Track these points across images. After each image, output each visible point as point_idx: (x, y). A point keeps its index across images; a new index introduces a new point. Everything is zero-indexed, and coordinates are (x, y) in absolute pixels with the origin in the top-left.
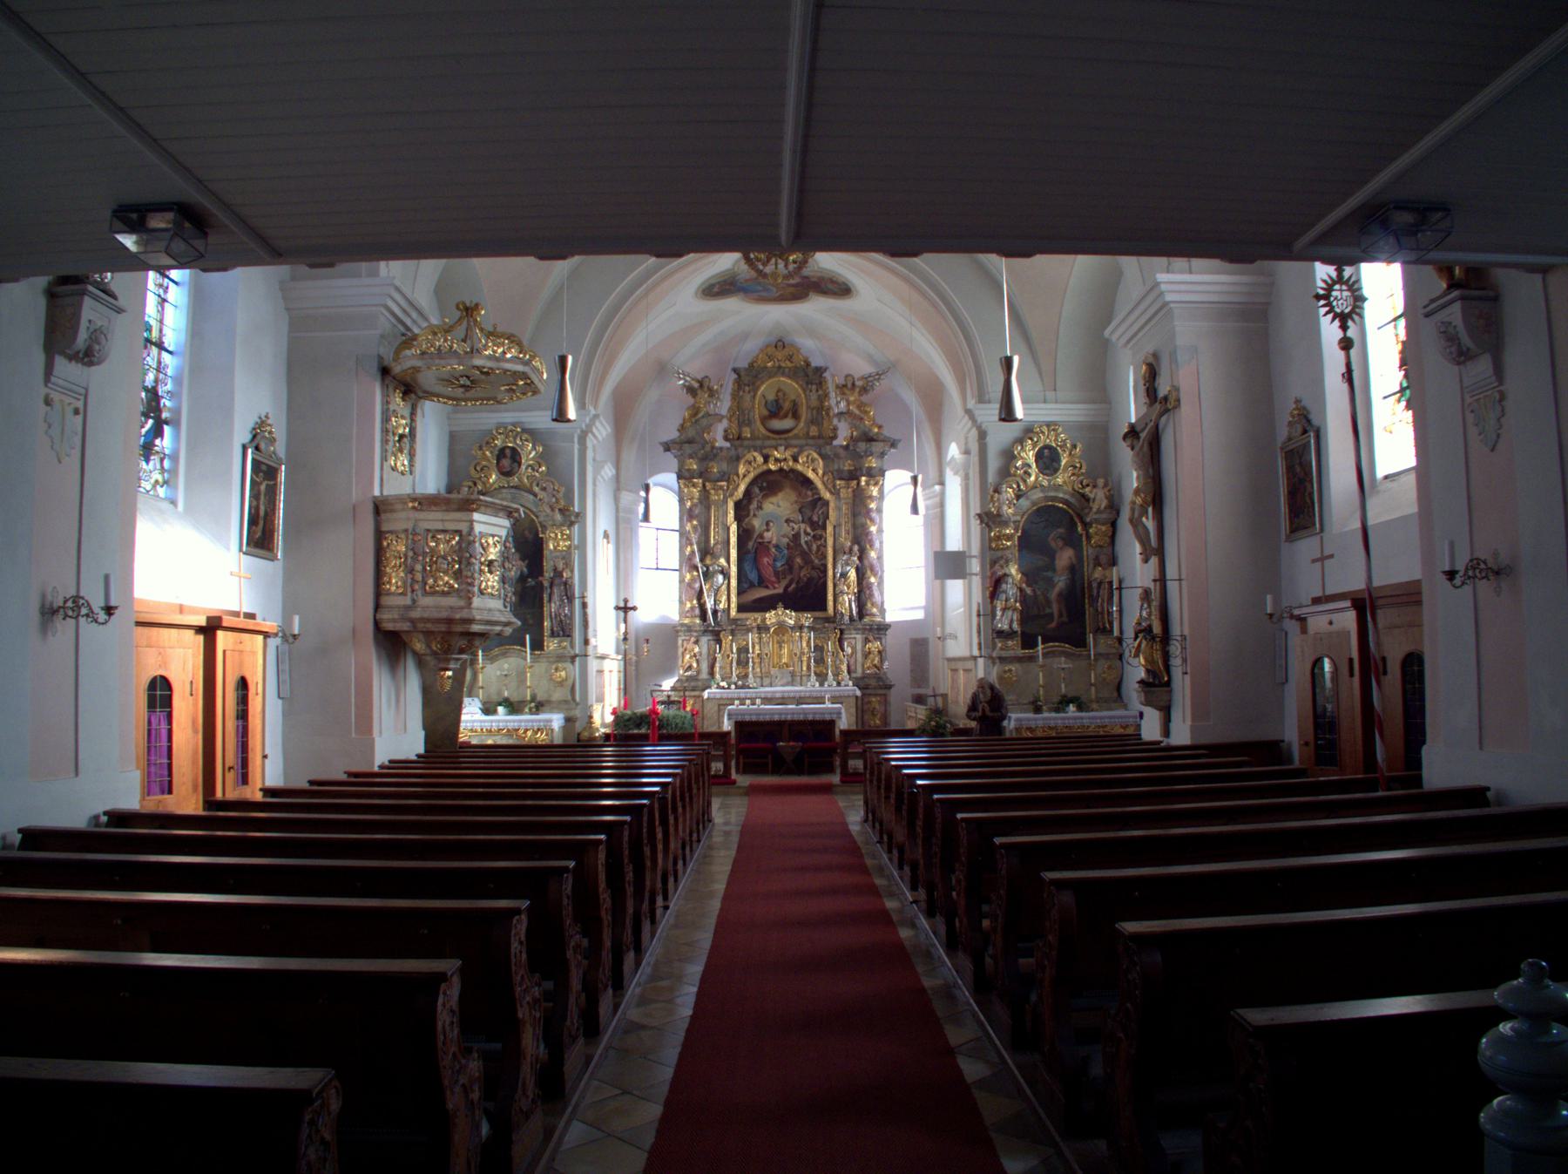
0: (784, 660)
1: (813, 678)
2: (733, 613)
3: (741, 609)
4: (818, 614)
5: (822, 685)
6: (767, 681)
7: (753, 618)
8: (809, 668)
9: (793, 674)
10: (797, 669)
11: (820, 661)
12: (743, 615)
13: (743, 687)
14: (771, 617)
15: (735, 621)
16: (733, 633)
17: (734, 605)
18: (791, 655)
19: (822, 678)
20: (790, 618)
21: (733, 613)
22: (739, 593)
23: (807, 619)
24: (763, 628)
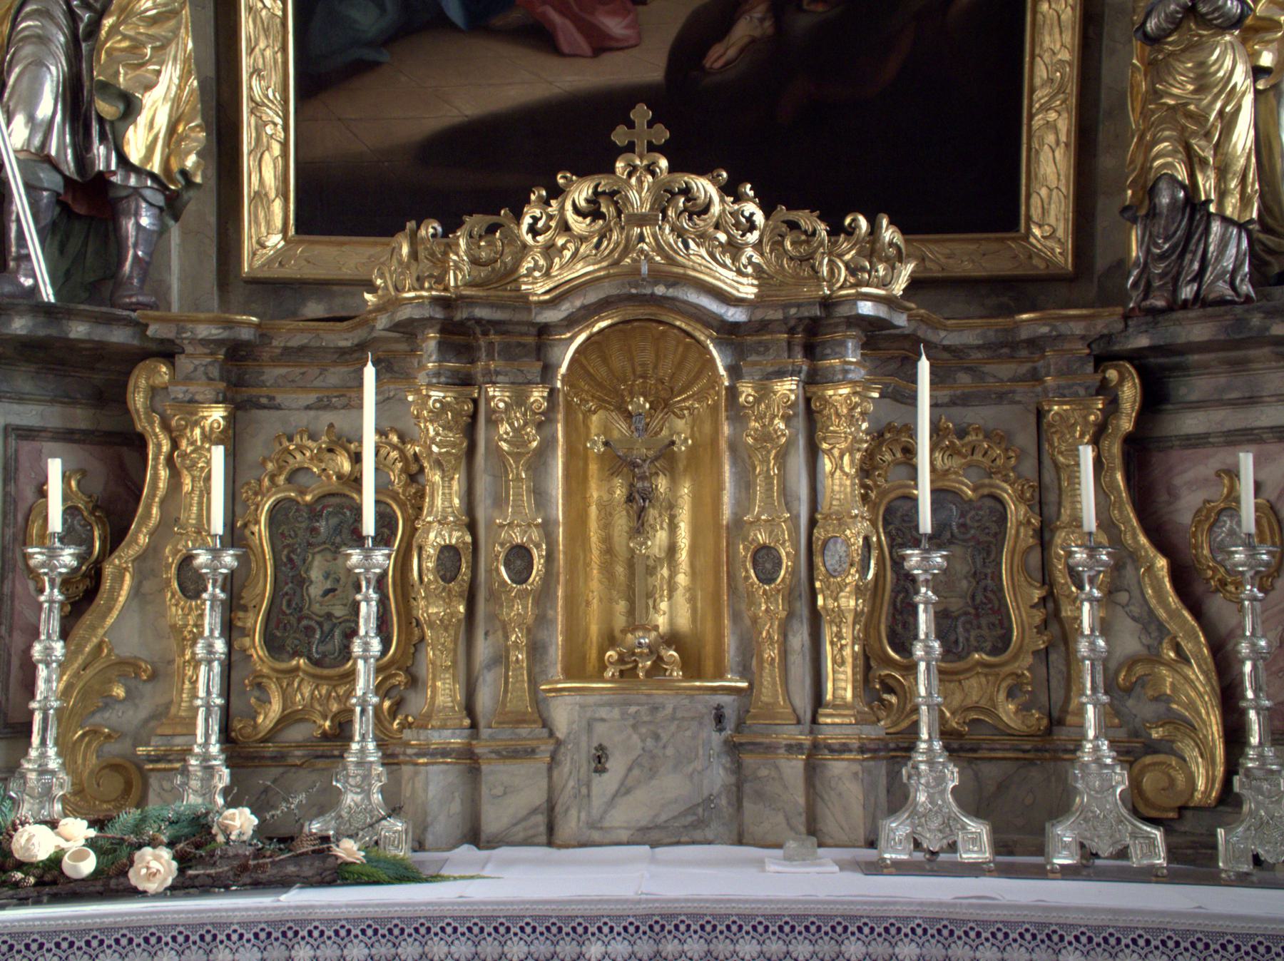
0: (671, 612)
1: (934, 777)
2: (267, 232)
3: (326, 202)
4: (963, 255)
5: (1019, 848)
6: (514, 791)
7: (400, 272)
8: (881, 681)
9: (741, 736)
10: (781, 692)
11: (975, 623)
12: (339, 257)
13: (250, 873)
14: (558, 247)
15: (277, 291)
16: (239, 373)
17: (267, 169)
18: (735, 563)
19: (1017, 784)
20: (727, 250)
21: (267, 232)
22: (316, 80)
23: (875, 268)
24: (484, 335)
